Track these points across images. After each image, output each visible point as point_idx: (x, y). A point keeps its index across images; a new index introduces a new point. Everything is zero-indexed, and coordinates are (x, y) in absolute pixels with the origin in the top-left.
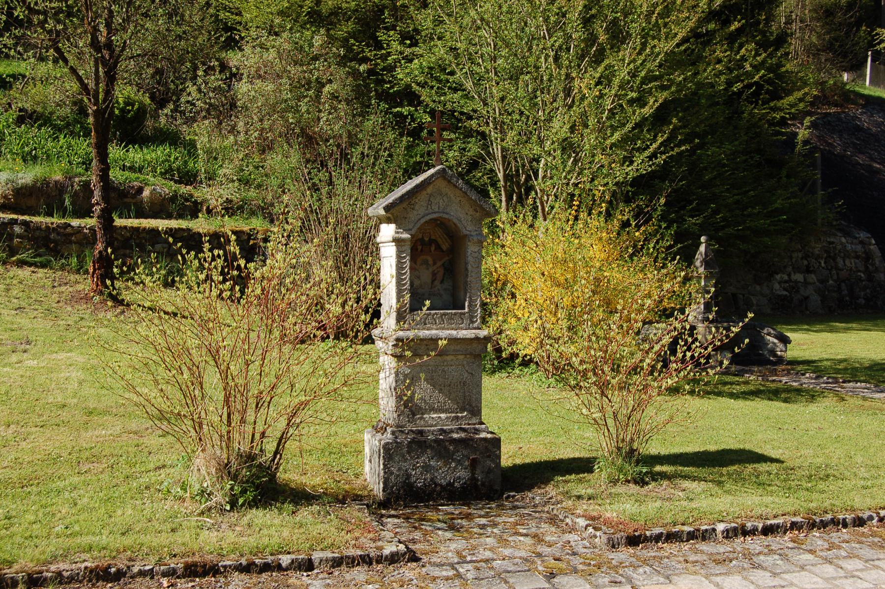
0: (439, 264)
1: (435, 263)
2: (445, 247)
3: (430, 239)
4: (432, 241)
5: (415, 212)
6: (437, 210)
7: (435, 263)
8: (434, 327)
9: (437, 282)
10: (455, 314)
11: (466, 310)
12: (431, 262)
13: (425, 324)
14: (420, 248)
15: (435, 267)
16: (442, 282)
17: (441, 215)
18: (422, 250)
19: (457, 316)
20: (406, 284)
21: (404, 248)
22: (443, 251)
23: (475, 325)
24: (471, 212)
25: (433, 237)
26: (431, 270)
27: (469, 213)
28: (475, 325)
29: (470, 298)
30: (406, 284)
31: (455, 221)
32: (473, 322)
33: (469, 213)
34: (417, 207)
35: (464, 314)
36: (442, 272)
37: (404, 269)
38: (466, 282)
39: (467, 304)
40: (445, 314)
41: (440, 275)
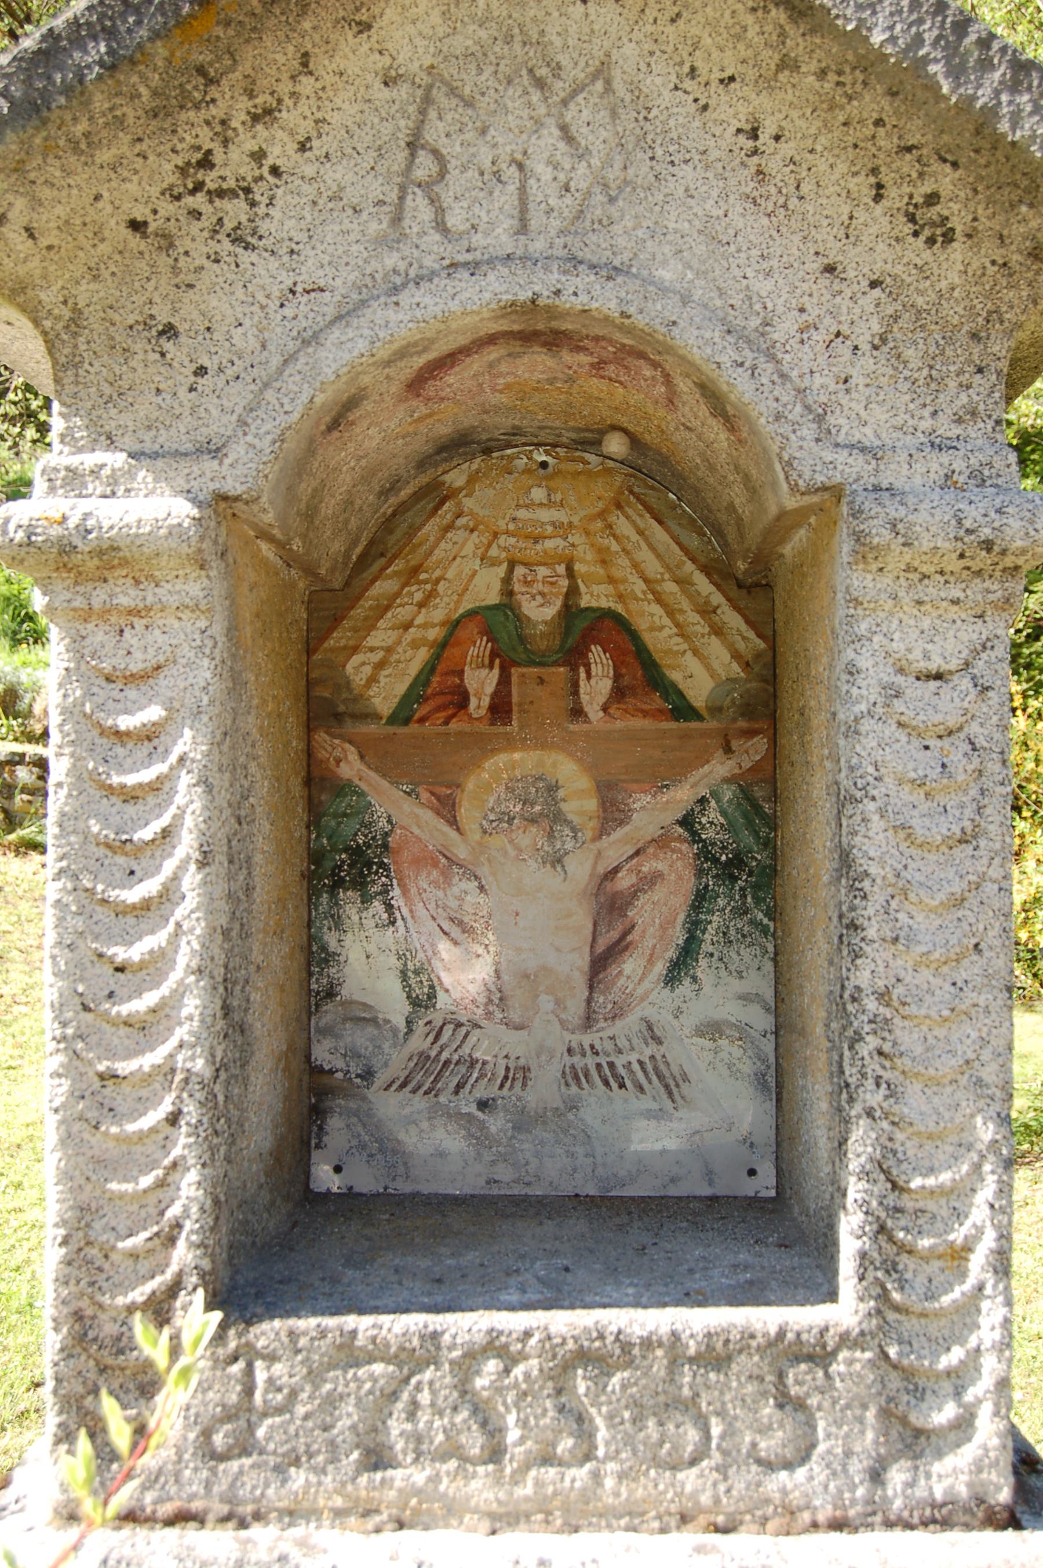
0: (653, 812)
1: (612, 813)
2: (703, 668)
3: (570, 611)
4: (586, 630)
5: (267, 273)
6: (501, 238)
7: (612, 813)
8: (480, 1487)
9: (638, 972)
10: (716, 1355)
11: (846, 1310)
12: (580, 803)
13: (377, 1458)
14: (481, 683)
15: (615, 847)
16: (681, 966)
17: (540, 284)
18: (500, 708)
19: (738, 1380)
20: (161, 1016)
21: (141, 648)
22: (682, 710)
23: (951, 1474)
24: (880, 243)
25: (595, 597)
26: (581, 868)
27: (859, 263)
28: (951, 1474)
29: (887, 1172)
30: (161, 1016)
31: (700, 342)
32: (915, 1442)
33: (859, 263)
34: (280, 222)
35: (817, 1353)
36: (676, 875)
37: (131, 856)
38: (843, 999)
39: (849, 1244)
40: (592, 1357)
41: (659, 914)
